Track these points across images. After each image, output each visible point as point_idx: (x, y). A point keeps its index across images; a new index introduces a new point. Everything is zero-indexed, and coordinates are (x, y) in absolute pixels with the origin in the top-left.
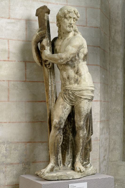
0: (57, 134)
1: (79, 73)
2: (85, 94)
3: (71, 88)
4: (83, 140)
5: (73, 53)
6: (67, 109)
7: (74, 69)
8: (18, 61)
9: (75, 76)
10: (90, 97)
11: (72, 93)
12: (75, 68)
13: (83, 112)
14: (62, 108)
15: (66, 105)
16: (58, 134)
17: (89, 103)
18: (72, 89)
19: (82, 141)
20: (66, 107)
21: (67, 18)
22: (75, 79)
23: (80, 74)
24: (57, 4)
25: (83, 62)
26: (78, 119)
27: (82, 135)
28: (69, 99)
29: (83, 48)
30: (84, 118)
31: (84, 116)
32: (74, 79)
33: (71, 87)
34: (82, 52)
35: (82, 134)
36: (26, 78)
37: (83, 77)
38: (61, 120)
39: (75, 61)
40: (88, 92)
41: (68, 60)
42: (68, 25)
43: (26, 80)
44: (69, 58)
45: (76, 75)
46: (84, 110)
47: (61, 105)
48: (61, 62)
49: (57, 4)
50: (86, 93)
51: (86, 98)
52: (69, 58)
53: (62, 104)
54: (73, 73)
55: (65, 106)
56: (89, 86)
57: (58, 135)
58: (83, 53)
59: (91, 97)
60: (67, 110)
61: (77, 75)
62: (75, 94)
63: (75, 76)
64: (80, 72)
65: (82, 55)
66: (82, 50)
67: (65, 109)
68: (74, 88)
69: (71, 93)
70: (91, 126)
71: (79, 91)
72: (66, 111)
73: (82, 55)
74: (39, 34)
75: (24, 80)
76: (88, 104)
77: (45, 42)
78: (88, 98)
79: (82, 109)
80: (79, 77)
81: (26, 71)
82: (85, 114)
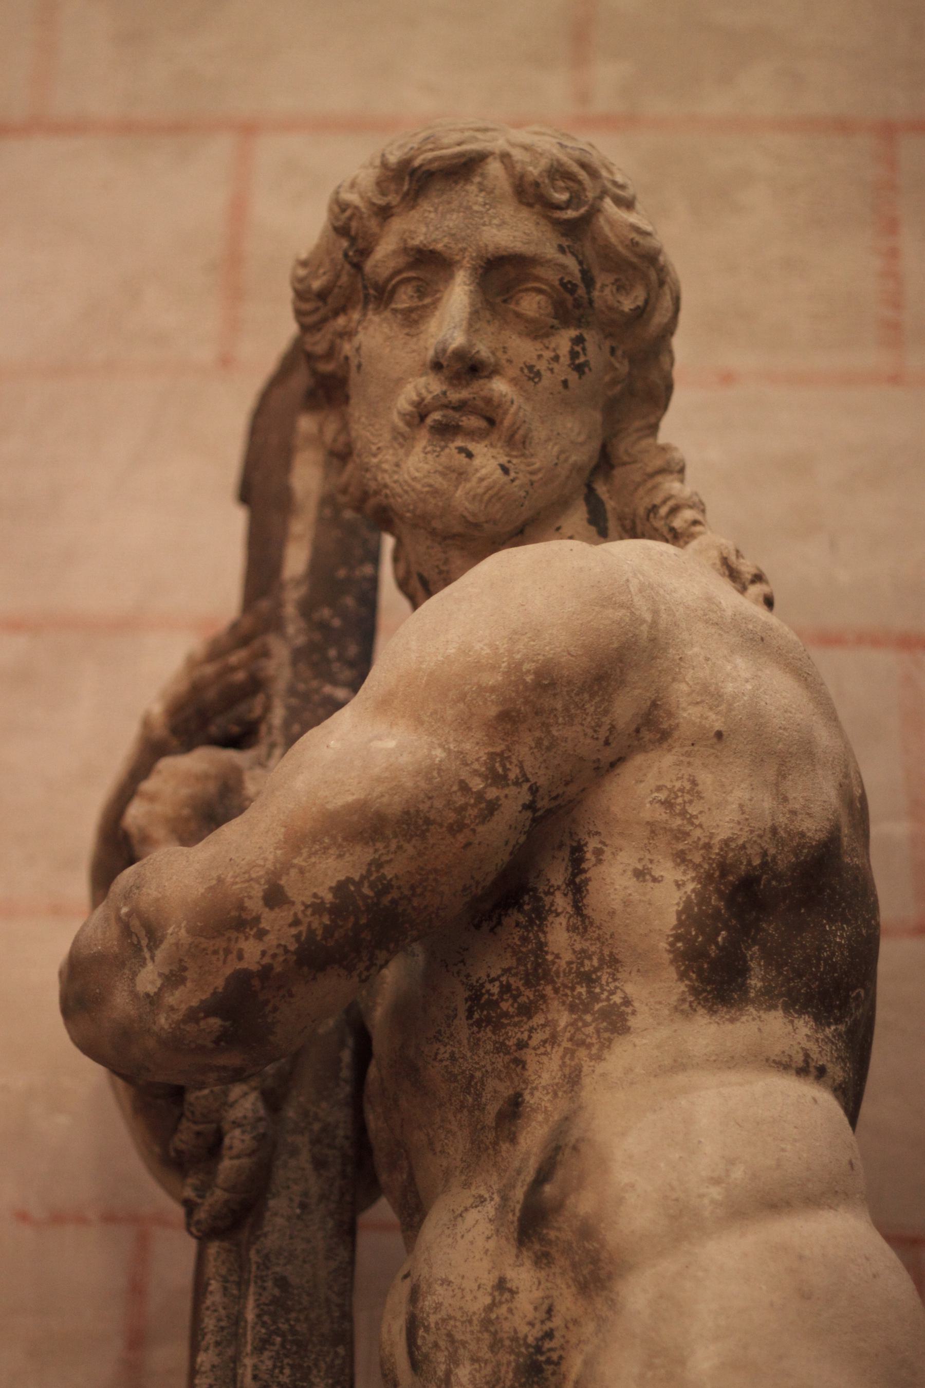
1: (561, 1231)
5: (361, 807)
7: (505, 1146)
8: (23, 1217)
9: (501, 1285)
12: (513, 1139)
21: (381, 295)
22: (496, 1345)
23: (587, 1231)
24: (727, 378)
25: (683, 1011)
29: (655, 726)
32: (485, 1353)
34: (653, 829)
37: (637, 1294)
39: (527, 1011)
41: (252, 953)
44: (275, 896)
45: (523, 1276)
48: (134, 995)
49: (727, 378)
52: (275, 896)
54: (485, 1228)
61: (543, 1260)
63: (501, 1285)
64: (584, 1204)
65: (640, 874)
73: (668, 871)
80: (567, 1303)
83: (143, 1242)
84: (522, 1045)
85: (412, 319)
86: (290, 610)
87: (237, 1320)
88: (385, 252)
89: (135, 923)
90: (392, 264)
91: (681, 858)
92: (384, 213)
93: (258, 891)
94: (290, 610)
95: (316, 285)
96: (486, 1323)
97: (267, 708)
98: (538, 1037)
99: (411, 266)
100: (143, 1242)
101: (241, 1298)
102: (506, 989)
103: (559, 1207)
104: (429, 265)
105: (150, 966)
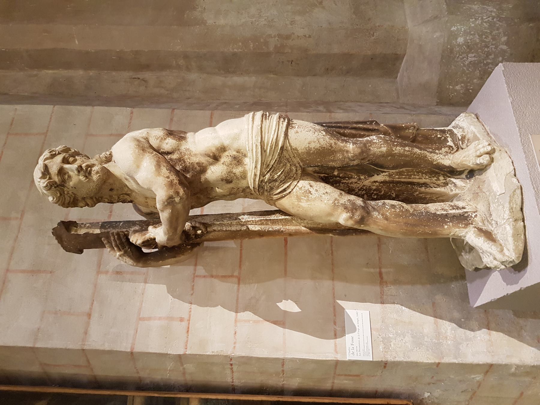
0: (380, 217)
1: (217, 154)
2: (272, 136)
3: (255, 175)
4: (397, 146)
5: (155, 166)
6: (311, 186)
10: (281, 123)
11: (268, 172)
13: (323, 142)
14: (308, 200)
15: (301, 189)
16: (379, 213)
17: (297, 127)
18: (258, 174)
19: (398, 148)
20: (306, 188)
26: (341, 157)
27: (384, 147)
28: (284, 182)
30: (338, 140)
31: (332, 142)
33: (253, 174)
35: (381, 147)
36: (232, 276)
37: (226, 143)
38: (342, 204)
39: (184, 162)
40: (267, 127)
42: (82, 178)
43: (236, 276)
44: (168, 177)
45: (222, 160)
46: (315, 140)
47: (300, 201)
50: (271, 133)
51: (283, 135)
52: (168, 177)
53: (299, 199)
55: (303, 193)
56: (250, 126)
57: (382, 215)
58: (163, 139)
59: (282, 120)
60: (315, 188)
62: (272, 163)
65: (167, 144)
66: (154, 143)
67: (310, 192)
68: (256, 167)
69: (267, 176)
70: (355, 125)
71: (263, 152)
72: (317, 191)
74: (120, 250)
75: (236, 280)
76: (299, 130)
77: (136, 239)
78: (284, 129)
79: (313, 146)
80: (226, 153)
81: (216, 277)
82: (327, 138)
83: (197, 276)
84: (189, 163)
85: (69, 177)
86: (106, 231)
87: (218, 225)
88: (56, 179)
89: (168, 201)
90: (59, 177)
91: (165, 139)
92: (50, 178)
93: (167, 179)
94: (106, 231)
95: (59, 195)
96: (228, 166)
97: (123, 232)
98: (189, 161)
99: (60, 175)
100: (197, 276)
101: (215, 224)
102: (181, 165)
103: (214, 153)
104: (61, 172)
105: (176, 199)
